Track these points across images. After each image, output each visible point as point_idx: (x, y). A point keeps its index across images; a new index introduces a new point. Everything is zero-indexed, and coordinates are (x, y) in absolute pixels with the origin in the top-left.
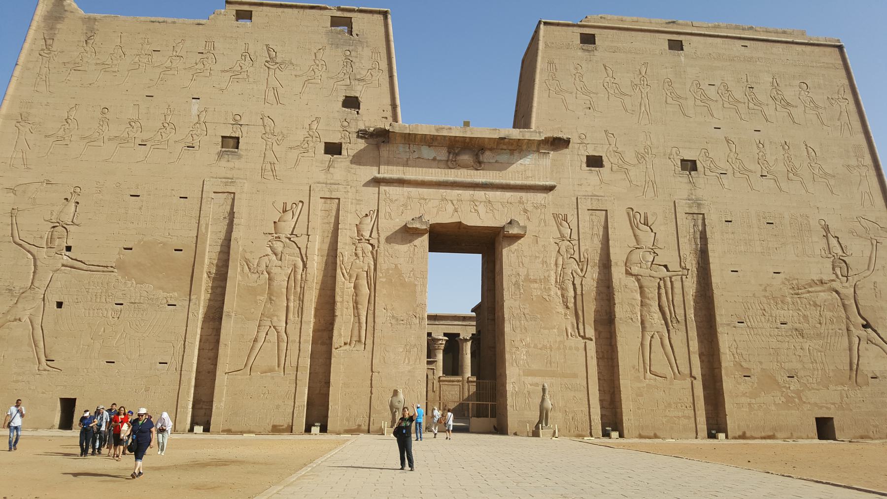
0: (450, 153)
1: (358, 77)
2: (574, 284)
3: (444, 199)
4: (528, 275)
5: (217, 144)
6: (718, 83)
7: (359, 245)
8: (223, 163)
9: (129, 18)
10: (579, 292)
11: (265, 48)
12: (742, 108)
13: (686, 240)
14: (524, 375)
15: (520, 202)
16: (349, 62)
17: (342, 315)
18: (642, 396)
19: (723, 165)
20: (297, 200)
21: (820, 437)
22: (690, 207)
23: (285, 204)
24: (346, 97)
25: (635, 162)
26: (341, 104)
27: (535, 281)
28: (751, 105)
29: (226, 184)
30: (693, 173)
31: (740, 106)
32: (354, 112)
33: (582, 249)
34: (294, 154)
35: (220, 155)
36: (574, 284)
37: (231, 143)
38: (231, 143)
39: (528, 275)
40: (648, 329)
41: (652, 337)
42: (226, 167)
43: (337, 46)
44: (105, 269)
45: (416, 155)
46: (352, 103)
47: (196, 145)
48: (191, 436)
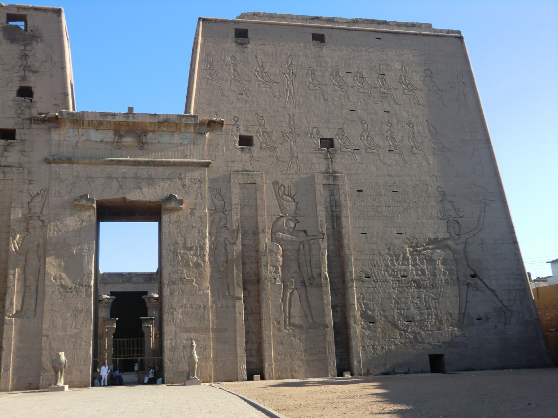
0: (115, 135)
1: (32, 69)
2: (226, 250)
3: (109, 178)
4: (185, 243)
6: (354, 70)
7: (31, 222)
10: (230, 257)
13: (323, 208)
14: (181, 332)
17: (14, 286)
18: (282, 344)
22: (328, 179)
27: (190, 249)
28: (382, 90)
30: (330, 149)
32: (28, 100)
33: (235, 218)
36: (226, 250)
39: (185, 243)
40: (289, 287)
41: (292, 294)
45: (84, 138)
46: (25, 92)
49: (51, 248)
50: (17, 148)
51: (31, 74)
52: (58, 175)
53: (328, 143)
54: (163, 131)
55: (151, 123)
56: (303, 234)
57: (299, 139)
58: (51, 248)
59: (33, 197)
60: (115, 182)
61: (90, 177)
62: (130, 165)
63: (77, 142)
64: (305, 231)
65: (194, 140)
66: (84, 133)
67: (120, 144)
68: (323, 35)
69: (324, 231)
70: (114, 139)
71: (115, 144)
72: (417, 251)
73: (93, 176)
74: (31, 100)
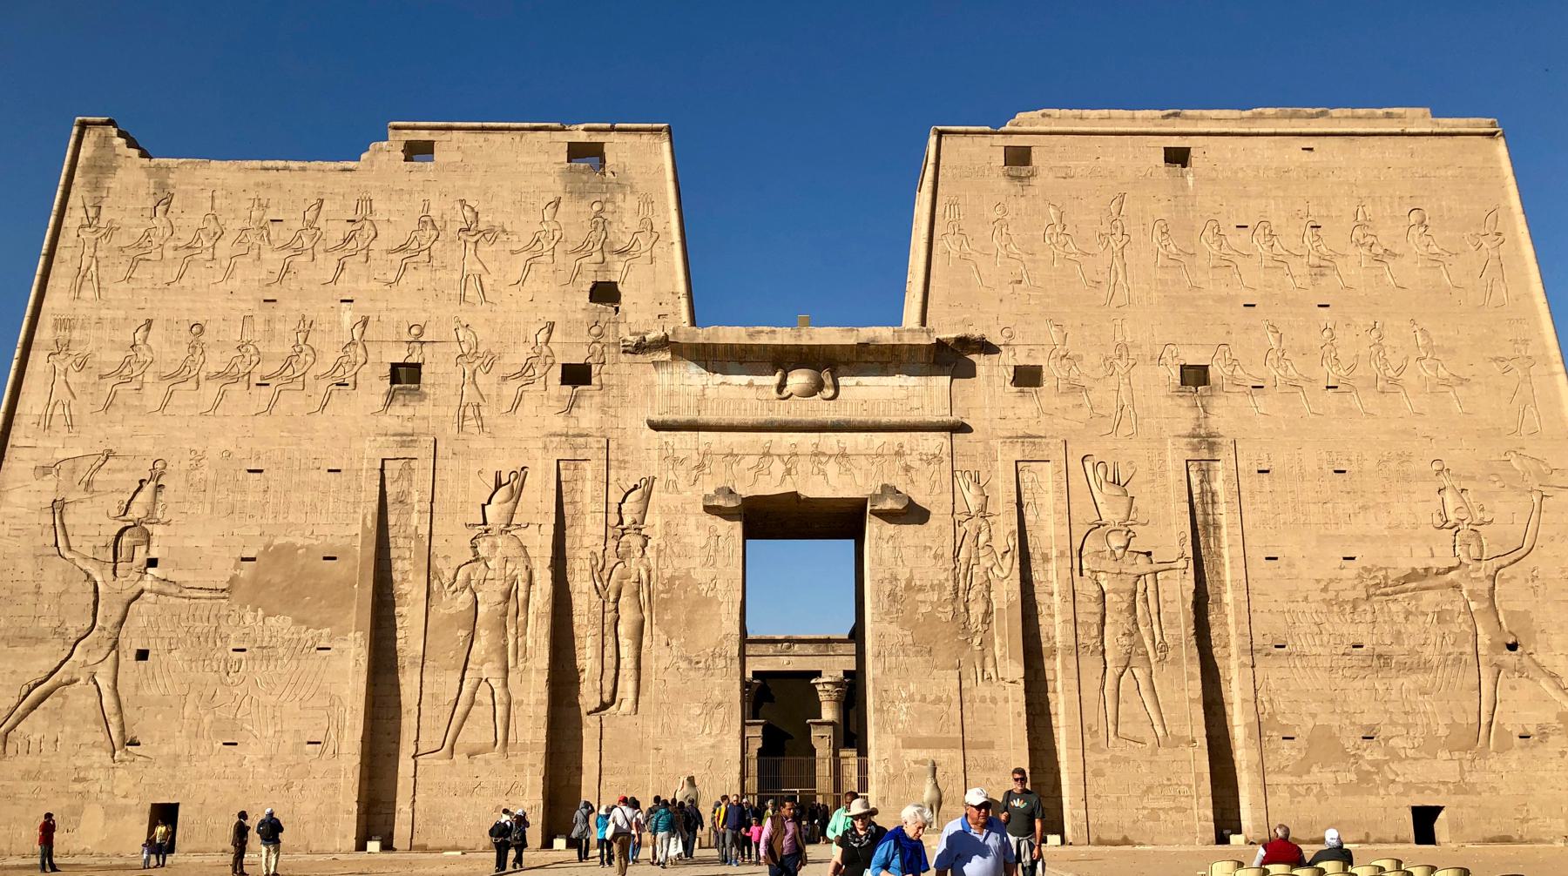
5: (381, 378)
8: (396, 409)
9: (226, 164)
11: (458, 206)
12: (1299, 267)
15: (897, 453)
16: (601, 221)
19: (1258, 372)
20: (516, 466)
21: (1418, 842)
23: (498, 476)
25: (1101, 372)
27: (921, 589)
28: (1314, 260)
29: (403, 445)
31: (1292, 261)
34: (511, 388)
35: (391, 397)
37: (405, 375)
38: (405, 375)
42: (402, 415)
43: (582, 195)
44: (214, 594)
46: (605, 293)
47: (349, 380)
48: (362, 855)
49: (661, 588)
50: (597, 399)
53: (1195, 376)
56: (1142, 559)
57: (1138, 372)
58: (661, 588)
61: (731, 454)
63: (704, 387)
64: (1149, 554)
68: (1188, 149)
69: (1189, 553)
72: (1387, 594)
74: (617, 310)
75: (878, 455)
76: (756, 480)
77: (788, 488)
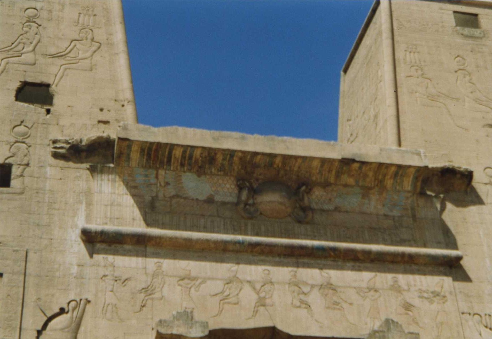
0: (241, 189)
1: (53, 50)
24: (25, 84)
26: (14, 93)
45: (171, 191)
46: (35, 93)
51: (50, 60)
52: (111, 269)
54: (346, 186)
55: (324, 161)
59: (50, 319)
60: (247, 289)
62: (279, 255)
63: (154, 200)
65: (413, 209)
66: (170, 181)
67: (252, 209)
70: (239, 196)
71: (242, 206)
73: (193, 274)
74: (48, 111)
75: (370, 289)
76: (220, 312)
77: (261, 321)
